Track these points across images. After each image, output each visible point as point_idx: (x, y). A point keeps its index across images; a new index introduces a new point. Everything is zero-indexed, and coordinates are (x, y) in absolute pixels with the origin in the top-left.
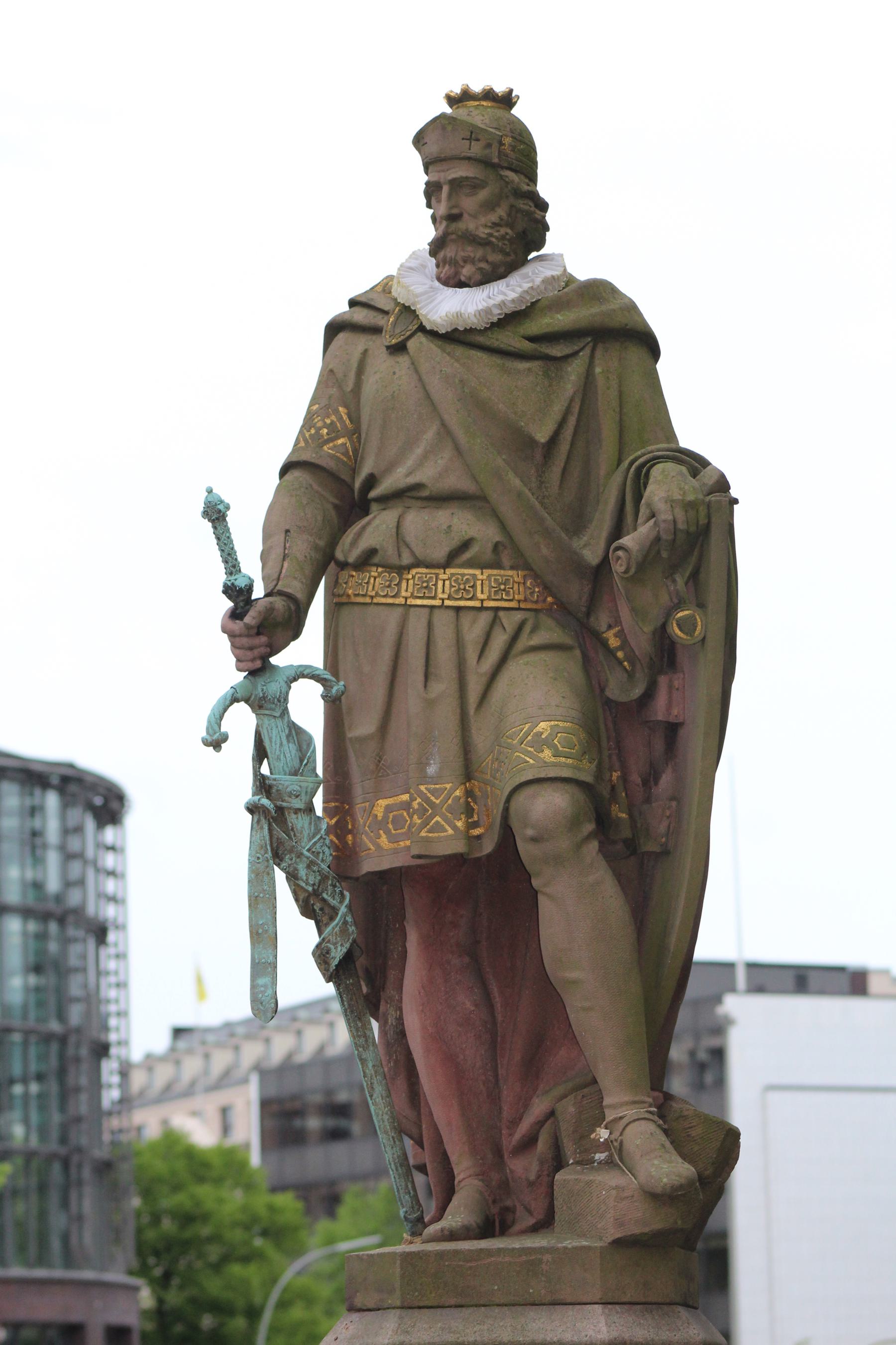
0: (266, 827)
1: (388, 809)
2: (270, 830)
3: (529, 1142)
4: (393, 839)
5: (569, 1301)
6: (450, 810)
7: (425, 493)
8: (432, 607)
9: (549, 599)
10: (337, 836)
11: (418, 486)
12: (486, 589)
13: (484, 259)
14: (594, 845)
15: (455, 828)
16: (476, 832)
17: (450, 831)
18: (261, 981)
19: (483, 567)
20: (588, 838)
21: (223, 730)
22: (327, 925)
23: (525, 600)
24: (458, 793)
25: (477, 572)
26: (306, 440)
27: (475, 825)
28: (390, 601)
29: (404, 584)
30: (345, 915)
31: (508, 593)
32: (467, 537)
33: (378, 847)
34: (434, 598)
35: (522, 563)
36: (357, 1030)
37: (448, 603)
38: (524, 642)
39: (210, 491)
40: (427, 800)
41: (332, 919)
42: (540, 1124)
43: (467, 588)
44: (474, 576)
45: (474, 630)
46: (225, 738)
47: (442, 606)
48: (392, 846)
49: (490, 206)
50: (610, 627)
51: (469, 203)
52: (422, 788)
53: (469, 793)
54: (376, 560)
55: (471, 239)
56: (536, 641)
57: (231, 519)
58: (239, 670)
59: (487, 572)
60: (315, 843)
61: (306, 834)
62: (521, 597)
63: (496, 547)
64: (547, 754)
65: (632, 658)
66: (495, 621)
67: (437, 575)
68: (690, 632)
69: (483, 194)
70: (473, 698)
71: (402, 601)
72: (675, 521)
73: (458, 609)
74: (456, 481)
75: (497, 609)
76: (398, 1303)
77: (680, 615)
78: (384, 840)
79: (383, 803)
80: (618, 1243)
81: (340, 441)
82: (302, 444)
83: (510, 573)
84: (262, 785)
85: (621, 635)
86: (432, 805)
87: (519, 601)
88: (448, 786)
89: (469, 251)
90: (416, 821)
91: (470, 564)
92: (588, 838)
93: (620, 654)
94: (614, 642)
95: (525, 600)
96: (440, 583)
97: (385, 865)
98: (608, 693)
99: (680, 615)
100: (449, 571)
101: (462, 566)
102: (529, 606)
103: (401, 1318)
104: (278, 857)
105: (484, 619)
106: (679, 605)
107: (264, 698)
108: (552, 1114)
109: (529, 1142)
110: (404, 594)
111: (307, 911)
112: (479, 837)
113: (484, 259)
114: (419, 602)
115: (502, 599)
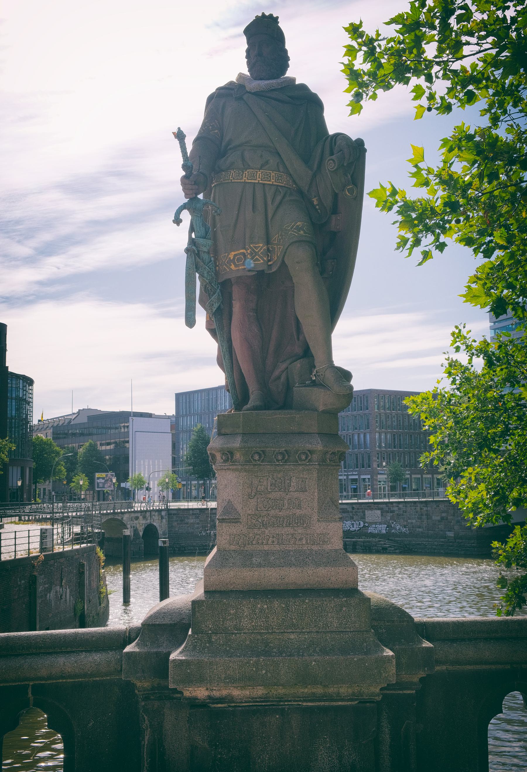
0: (193, 256)
1: (235, 255)
2: (195, 258)
4: (236, 266)
5: (305, 432)
8: (254, 183)
9: (294, 186)
12: (274, 178)
15: (263, 260)
16: (270, 263)
17: (262, 261)
18: (189, 313)
22: (212, 295)
26: (203, 130)
27: (269, 261)
28: (239, 181)
29: (244, 175)
34: (256, 180)
36: (221, 334)
37: (260, 182)
40: (253, 250)
41: (214, 294)
42: (283, 372)
46: (181, 221)
48: (236, 269)
52: (251, 246)
53: (268, 249)
58: (186, 198)
64: (302, 232)
67: (257, 172)
70: (270, 215)
71: (243, 180)
75: (278, 186)
76: (241, 432)
78: (233, 267)
79: (233, 253)
81: (216, 131)
82: (202, 131)
84: (192, 241)
88: (261, 245)
90: (243, 261)
94: (315, 203)
96: (258, 174)
103: (243, 437)
104: (197, 269)
108: (287, 368)
112: (270, 265)
115: (279, 182)
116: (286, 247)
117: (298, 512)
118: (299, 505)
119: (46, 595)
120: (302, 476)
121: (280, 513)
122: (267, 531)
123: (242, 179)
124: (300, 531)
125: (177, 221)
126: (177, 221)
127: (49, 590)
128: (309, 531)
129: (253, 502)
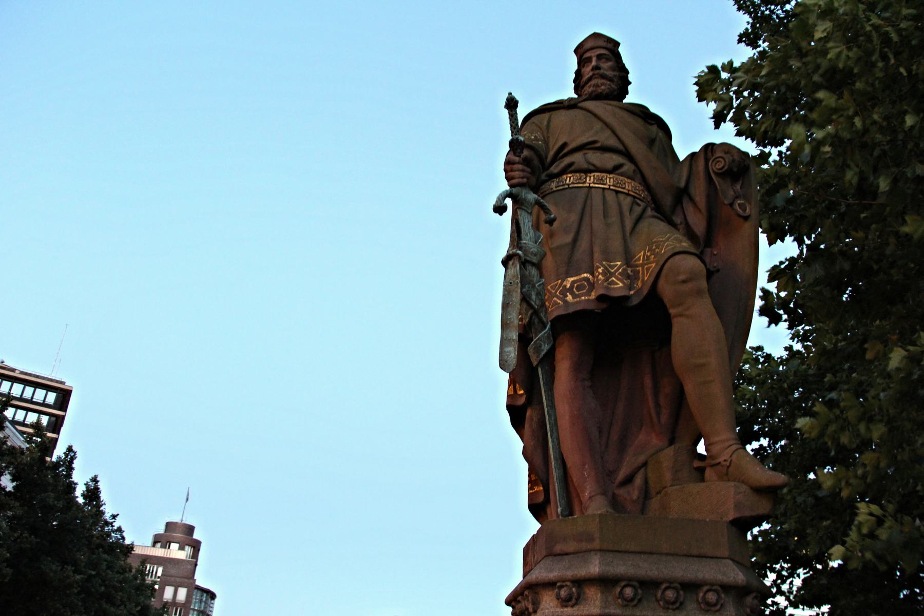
1: (573, 282)
3: (629, 480)
5: (709, 555)
6: (620, 274)
7: (598, 145)
8: (604, 189)
11: (595, 142)
17: (621, 285)
33: (566, 302)
39: (510, 94)
47: (609, 189)
54: (573, 168)
55: (603, 77)
74: (612, 142)
76: (598, 547)
78: (569, 298)
79: (571, 279)
86: (610, 272)
88: (619, 263)
89: (603, 81)
97: (571, 310)
101: (618, 174)
106: (737, 197)
109: (629, 480)
110: (588, 181)
116: (661, 263)
123: (585, 182)
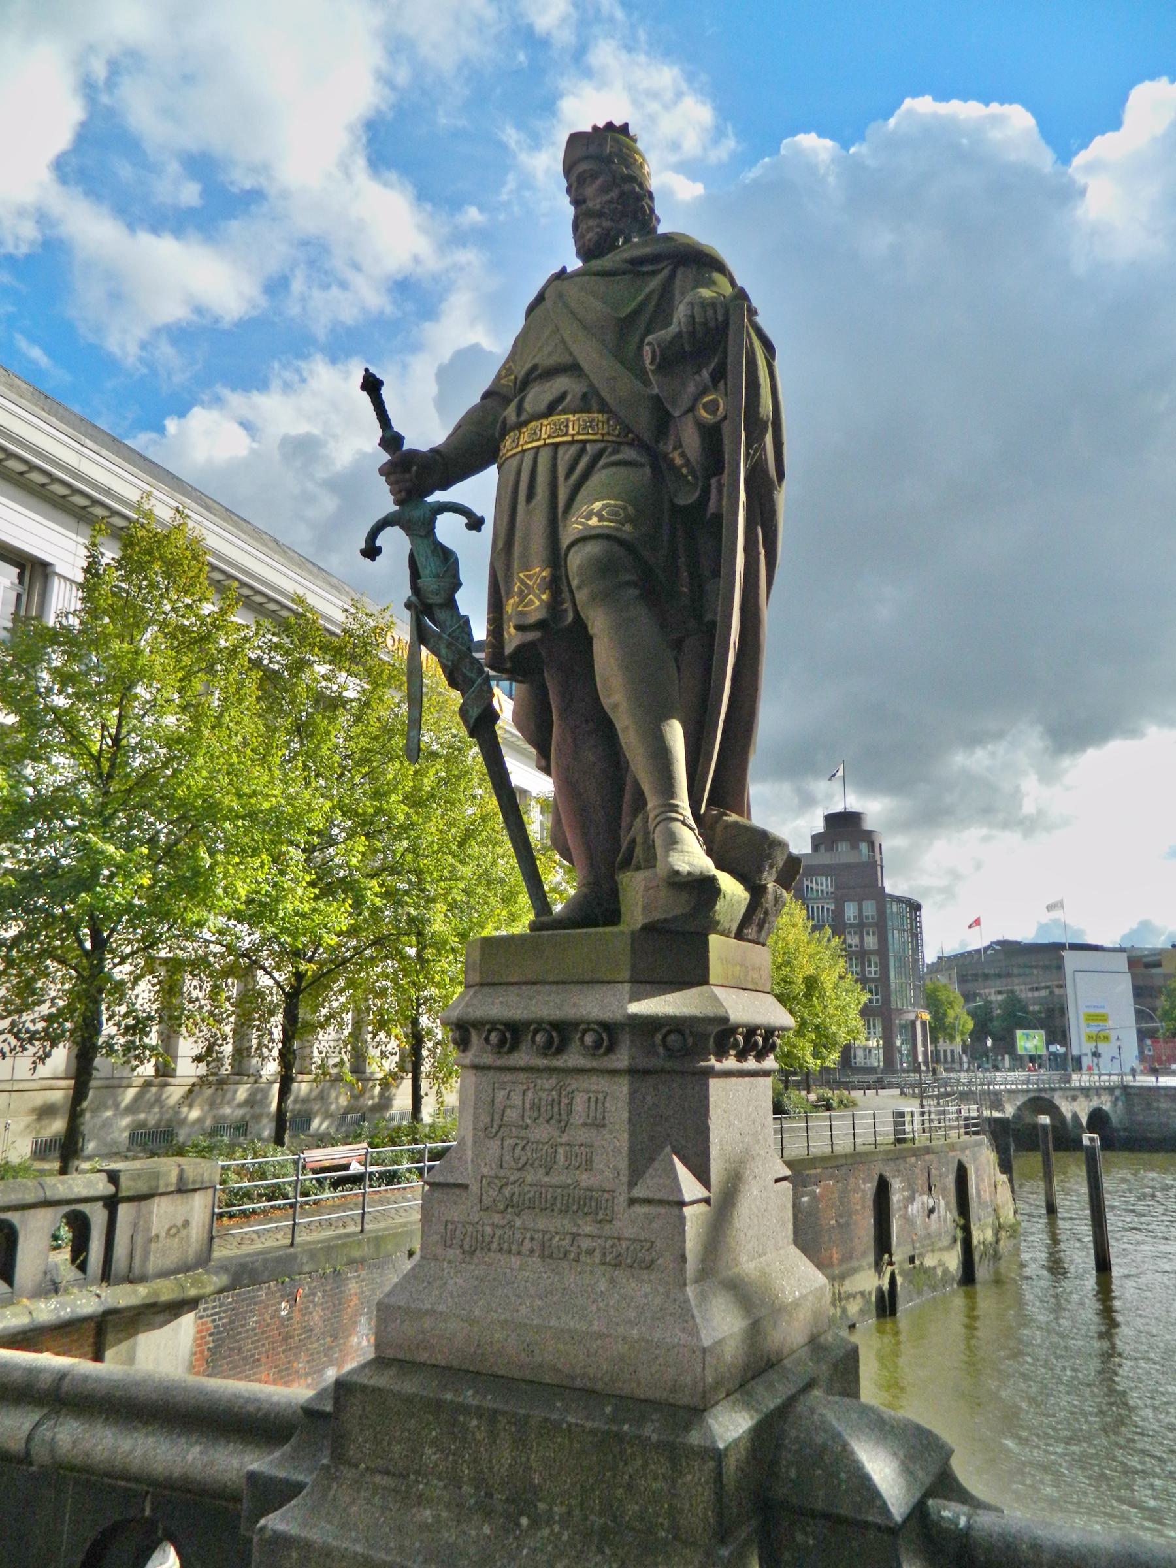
8: (538, 448)
10: (495, 638)
12: (576, 428)
13: (599, 226)
14: (634, 592)
19: (574, 413)
20: (629, 584)
21: (377, 544)
23: (608, 434)
24: (544, 574)
25: (570, 417)
30: (480, 685)
31: (593, 429)
32: (563, 389)
35: (604, 408)
37: (548, 441)
38: (602, 462)
43: (563, 428)
44: (568, 420)
45: (565, 457)
47: (545, 444)
49: (605, 189)
50: (675, 448)
51: (590, 191)
56: (614, 458)
57: (385, 392)
59: (577, 416)
60: (454, 631)
61: (448, 624)
62: (605, 431)
63: (585, 396)
65: (692, 472)
66: (583, 451)
68: (714, 412)
69: (599, 182)
72: (693, 317)
73: (556, 446)
75: (584, 442)
77: (705, 400)
80: (648, 928)
83: (596, 415)
85: (683, 455)
86: (527, 586)
87: (603, 435)
91: (564, 412)
92: (629, 584)
93: (684, 471)
94: (678, 461)
95: (608, 434)
98: (676, 501)
99: (705, 400)
100: (550, 419)
101: (559, 414)
102: (610, 438)
105: (573, 450)
106: (703, 393)
107: (409, 521)
111: (453, 683)
113: (598, 226)
114: (530, 446)
115: (588, 434)
117: (586, 1180)
118: (589, 1161)
119: (906, 1208)
120: (594, 1088)
121: (546, 1179)
122: (518, 1223)
123: (517, 446)
124: (588, 1229)
125: (371, 551)
126: (371, 551)
127: (912, 1199)
128: (607, 1230)
129: (494, 1146)
